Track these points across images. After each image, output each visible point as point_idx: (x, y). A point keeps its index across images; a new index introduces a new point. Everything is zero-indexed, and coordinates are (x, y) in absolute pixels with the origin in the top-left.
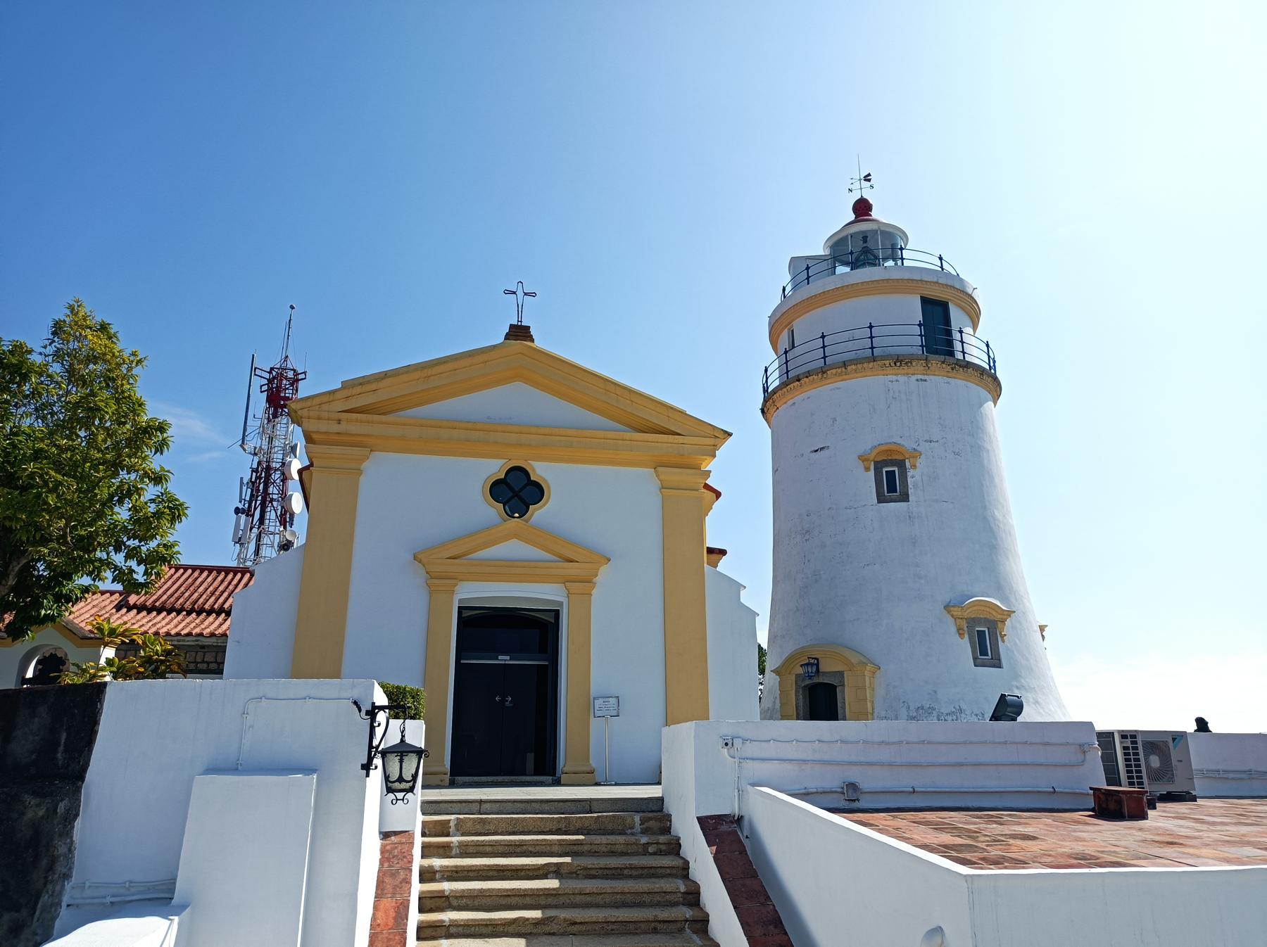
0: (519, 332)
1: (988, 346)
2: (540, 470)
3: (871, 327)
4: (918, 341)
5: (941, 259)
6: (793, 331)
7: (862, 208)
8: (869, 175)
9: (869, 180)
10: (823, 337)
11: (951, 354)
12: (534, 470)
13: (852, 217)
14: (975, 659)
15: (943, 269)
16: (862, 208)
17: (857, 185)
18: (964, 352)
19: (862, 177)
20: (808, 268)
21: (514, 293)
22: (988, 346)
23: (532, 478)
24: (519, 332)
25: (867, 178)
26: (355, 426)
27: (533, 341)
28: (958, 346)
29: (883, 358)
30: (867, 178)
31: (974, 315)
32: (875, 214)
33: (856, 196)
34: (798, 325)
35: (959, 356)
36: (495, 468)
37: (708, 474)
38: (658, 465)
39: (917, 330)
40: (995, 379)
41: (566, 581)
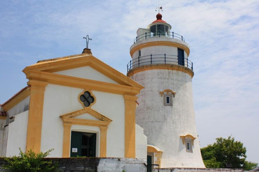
0: (87, 51)
1: (192, 63)
2: (94, 93)
3: (165, 55)
4: (177, 61)
5: (182, 37)
6: (140, 52)
7: (159, 17)
8: (162, 7)
9: (162, 9)
10: (151, 55)
11: (184, 65)
12: (92, 93)
13: (156, 19)
14: (187, 150)
15: (182, 40)
16: (159, 17)
17: (158, 10)
18: (188, 65)
19: (160, 8)
20: (146, 33)
21: (86, 38)
22: (192, 63)
23: (91, 95)
24: (87, 51)
25: (161, 8)
26: (44, 76)
27: (92, 54)
28: (186, 63)
29: (169, 65)
30: (161, 8)
31: (188, 55)
32: (162, 19)
33: (157, 13)
34: (143, 51)
35: (186, 66)
36: (80, 91)
37: (137, 98)
38: (125, 94)
39: (177, 58)
40: (193, 73)
41: (100, 126)
